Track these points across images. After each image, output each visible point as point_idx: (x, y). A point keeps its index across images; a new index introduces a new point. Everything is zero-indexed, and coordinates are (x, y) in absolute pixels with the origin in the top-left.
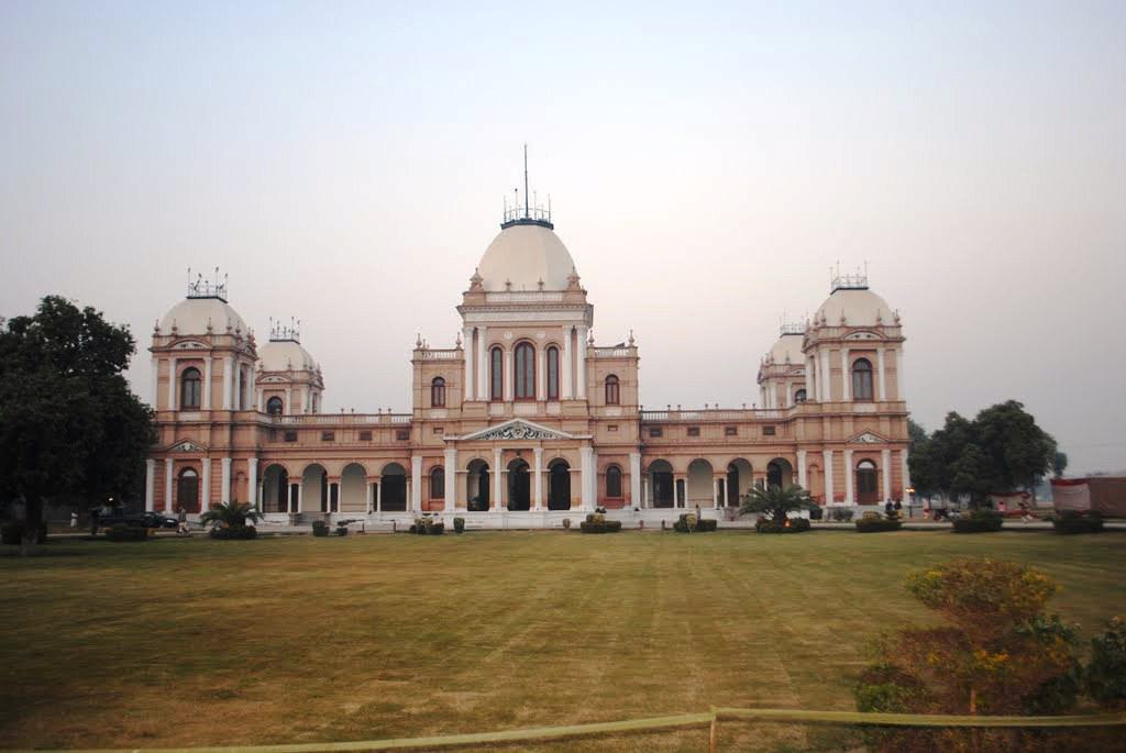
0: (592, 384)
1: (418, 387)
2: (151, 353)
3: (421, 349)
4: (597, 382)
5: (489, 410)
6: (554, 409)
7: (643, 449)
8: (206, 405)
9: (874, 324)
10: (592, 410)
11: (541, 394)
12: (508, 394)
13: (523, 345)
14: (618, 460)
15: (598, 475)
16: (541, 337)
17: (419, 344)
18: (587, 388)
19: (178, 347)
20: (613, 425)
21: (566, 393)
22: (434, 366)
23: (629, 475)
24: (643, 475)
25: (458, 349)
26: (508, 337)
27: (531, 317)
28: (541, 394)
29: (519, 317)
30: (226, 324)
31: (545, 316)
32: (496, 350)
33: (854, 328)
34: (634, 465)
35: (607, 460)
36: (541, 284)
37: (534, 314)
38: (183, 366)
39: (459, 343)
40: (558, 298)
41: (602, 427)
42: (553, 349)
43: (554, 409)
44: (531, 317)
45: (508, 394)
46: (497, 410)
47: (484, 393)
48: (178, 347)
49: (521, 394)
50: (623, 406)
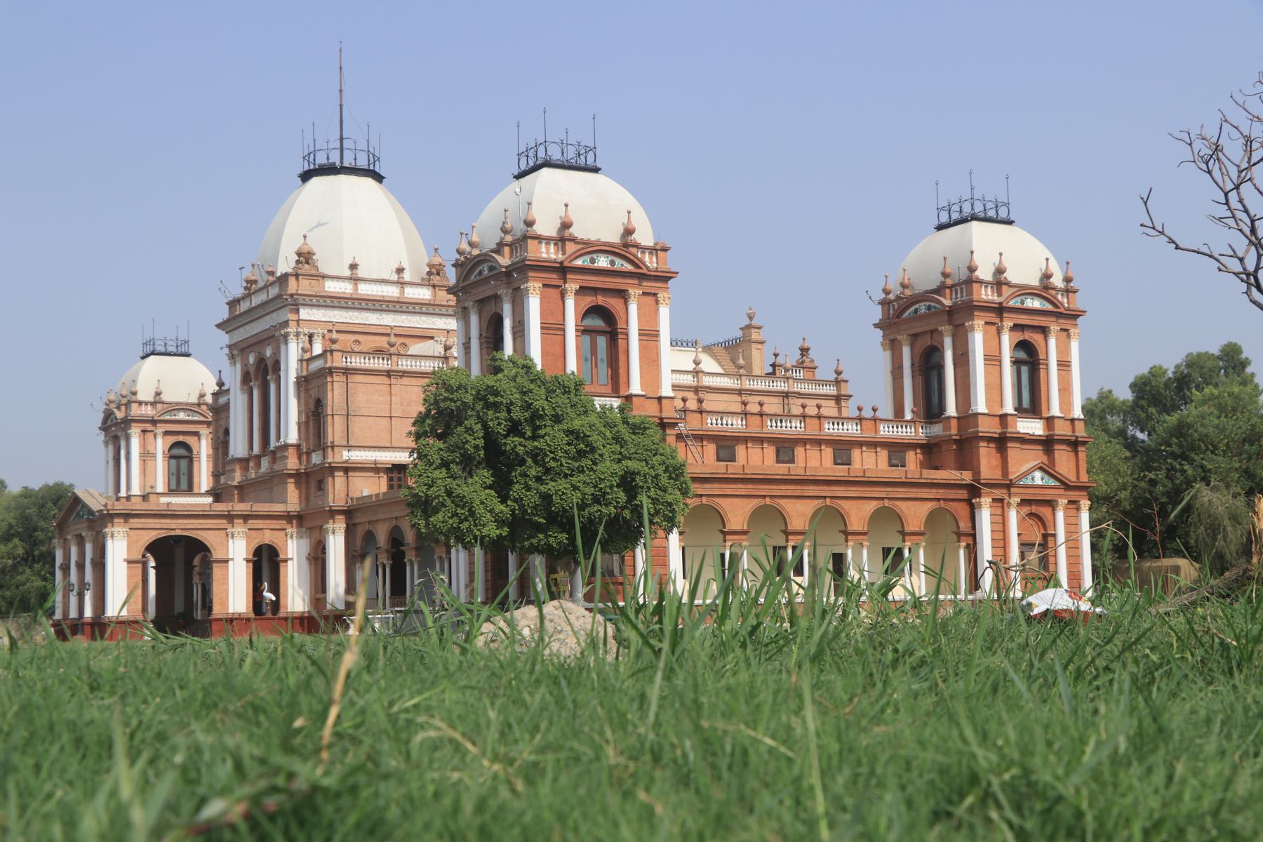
8: (123, 493)
9: (612, 236)
26: (251, 360)
33: (587, 243)
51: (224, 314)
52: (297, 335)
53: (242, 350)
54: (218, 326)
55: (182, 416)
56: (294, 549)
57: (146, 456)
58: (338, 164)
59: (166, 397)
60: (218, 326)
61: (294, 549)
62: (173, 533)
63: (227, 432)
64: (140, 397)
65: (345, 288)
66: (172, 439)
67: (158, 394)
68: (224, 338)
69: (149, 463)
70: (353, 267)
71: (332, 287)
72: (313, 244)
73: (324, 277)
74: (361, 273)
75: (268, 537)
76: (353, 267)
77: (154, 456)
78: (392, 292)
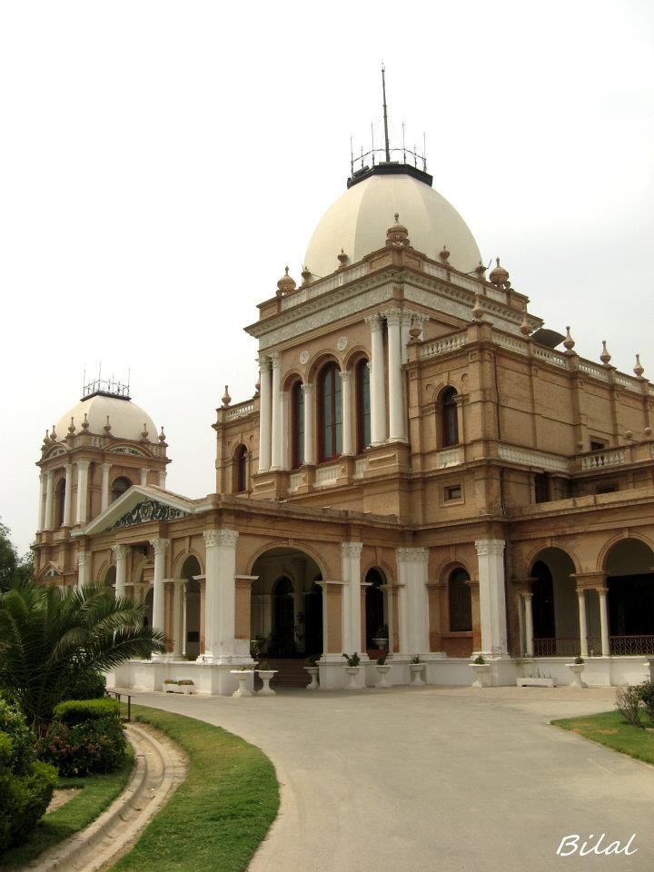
0: (414, 412)
1: (222, 465)
2: (39, 469)
3: (225, 410)
4: (421, 407)
5: (289, 486)
6: (363, 470)
7: (509, 528)
8: (65, 523)
10: (417, 462)
11: (346, 447)
12: (308, 457)
13: (325, 369)
14: (461, 557)
15: (430, 587)
16: (341, 347)
17: (227, 400)
18: (407, 422)
19: (51, 457)
20: (452, 486)
21: (375, 438)
22: (236, 429)
23: (477, 584)
24: (511, 582)
25: (257, 396)
26: (304, 359)
27: (327, 317)
28: (346, 447)
29: (315, 322)
30: (83, 421)
31: (345, 309)
32: (293, 386)
34: (488, 568)
35: (443, 557)
36: (343, 258)
37: (331, 311)
38: (58, 478)
39: (258, 387)
40: (362, 272)
41: (435, 492)
42: (359, 364)
43: (363, 470)
44: (327, 317)
45: (308, 457)
46: (298, 484)
47: (280, 461)
48: (51, 457)
49: (329, 452)
50: (465, 446)
51: (255, 317)
52: (401, 316)
53: (284, 352)
54: (247, 329)
55: (127, 452)
56: (413, 575)
57: (93, 489)
58: (401, 162)
59: (115, 433)
60: (247, 329)
61: (413, 575)
62: (283, 545)
63: (242, 449)
64: (92, 429)
65: (440, 274)
66: (117, 474)
67: (107, 428)
68: (254, 344)
69: (95, 496)
70: (445, 255)
71: (428, 270)
72: (403, 223)
73: (423, 257)
74: (451, 260)
75: (380, 558)
76: (445, 255)
77: (100, 488)
78: (477, 290)
